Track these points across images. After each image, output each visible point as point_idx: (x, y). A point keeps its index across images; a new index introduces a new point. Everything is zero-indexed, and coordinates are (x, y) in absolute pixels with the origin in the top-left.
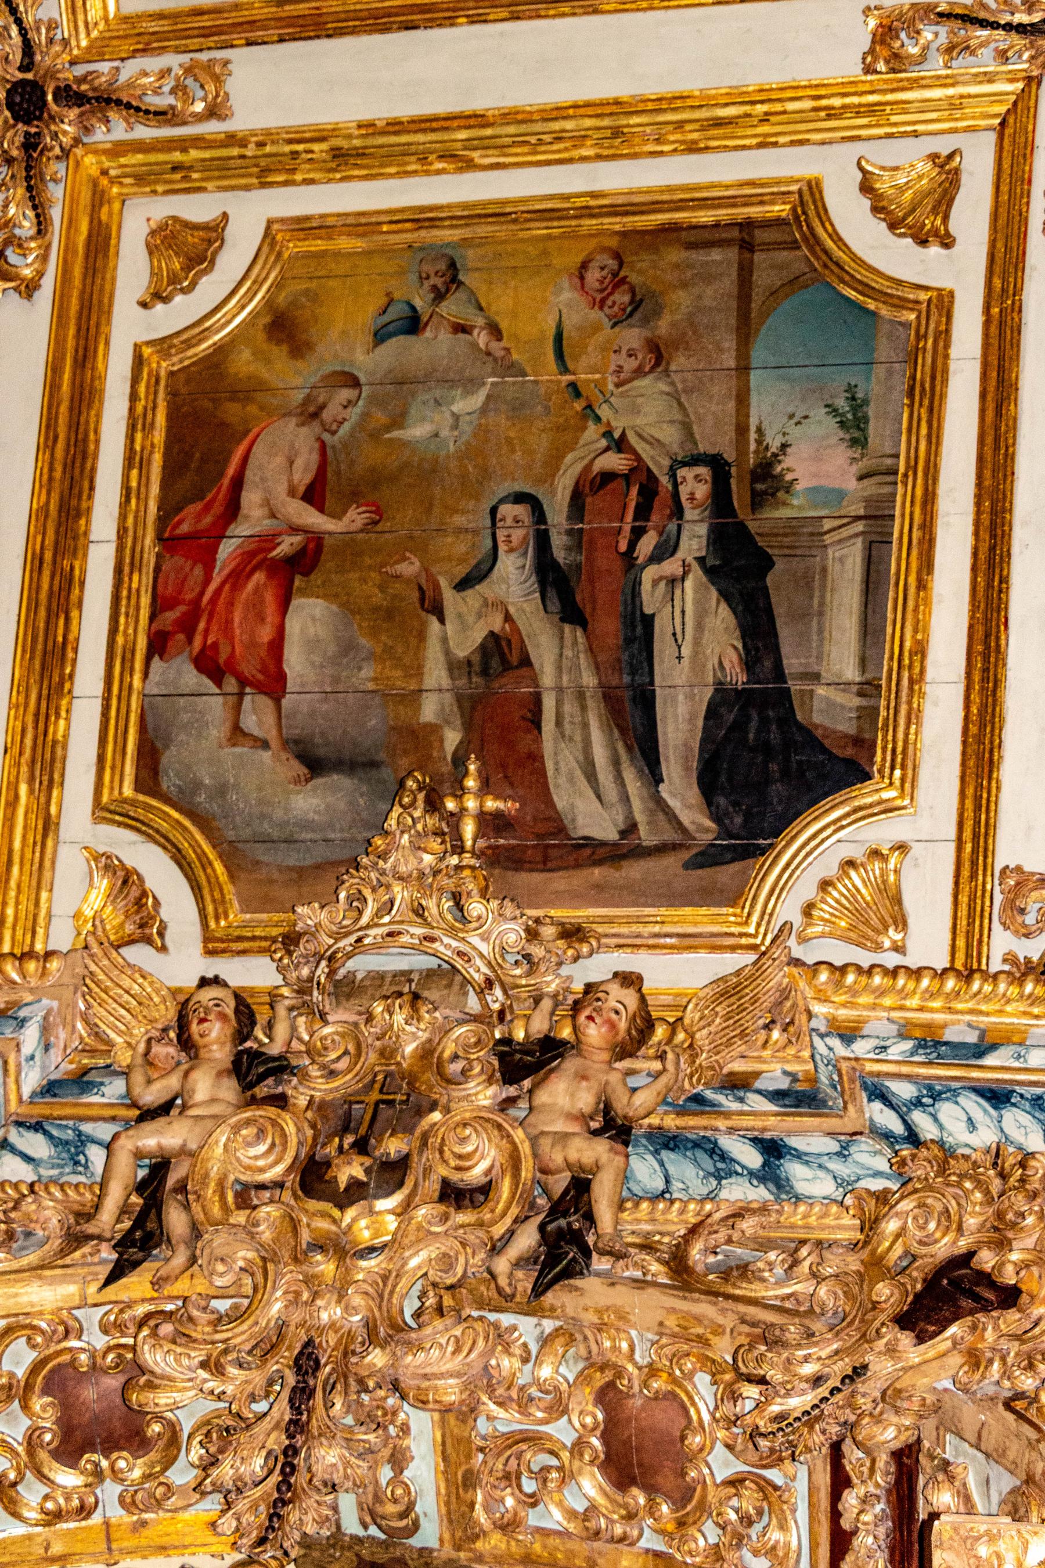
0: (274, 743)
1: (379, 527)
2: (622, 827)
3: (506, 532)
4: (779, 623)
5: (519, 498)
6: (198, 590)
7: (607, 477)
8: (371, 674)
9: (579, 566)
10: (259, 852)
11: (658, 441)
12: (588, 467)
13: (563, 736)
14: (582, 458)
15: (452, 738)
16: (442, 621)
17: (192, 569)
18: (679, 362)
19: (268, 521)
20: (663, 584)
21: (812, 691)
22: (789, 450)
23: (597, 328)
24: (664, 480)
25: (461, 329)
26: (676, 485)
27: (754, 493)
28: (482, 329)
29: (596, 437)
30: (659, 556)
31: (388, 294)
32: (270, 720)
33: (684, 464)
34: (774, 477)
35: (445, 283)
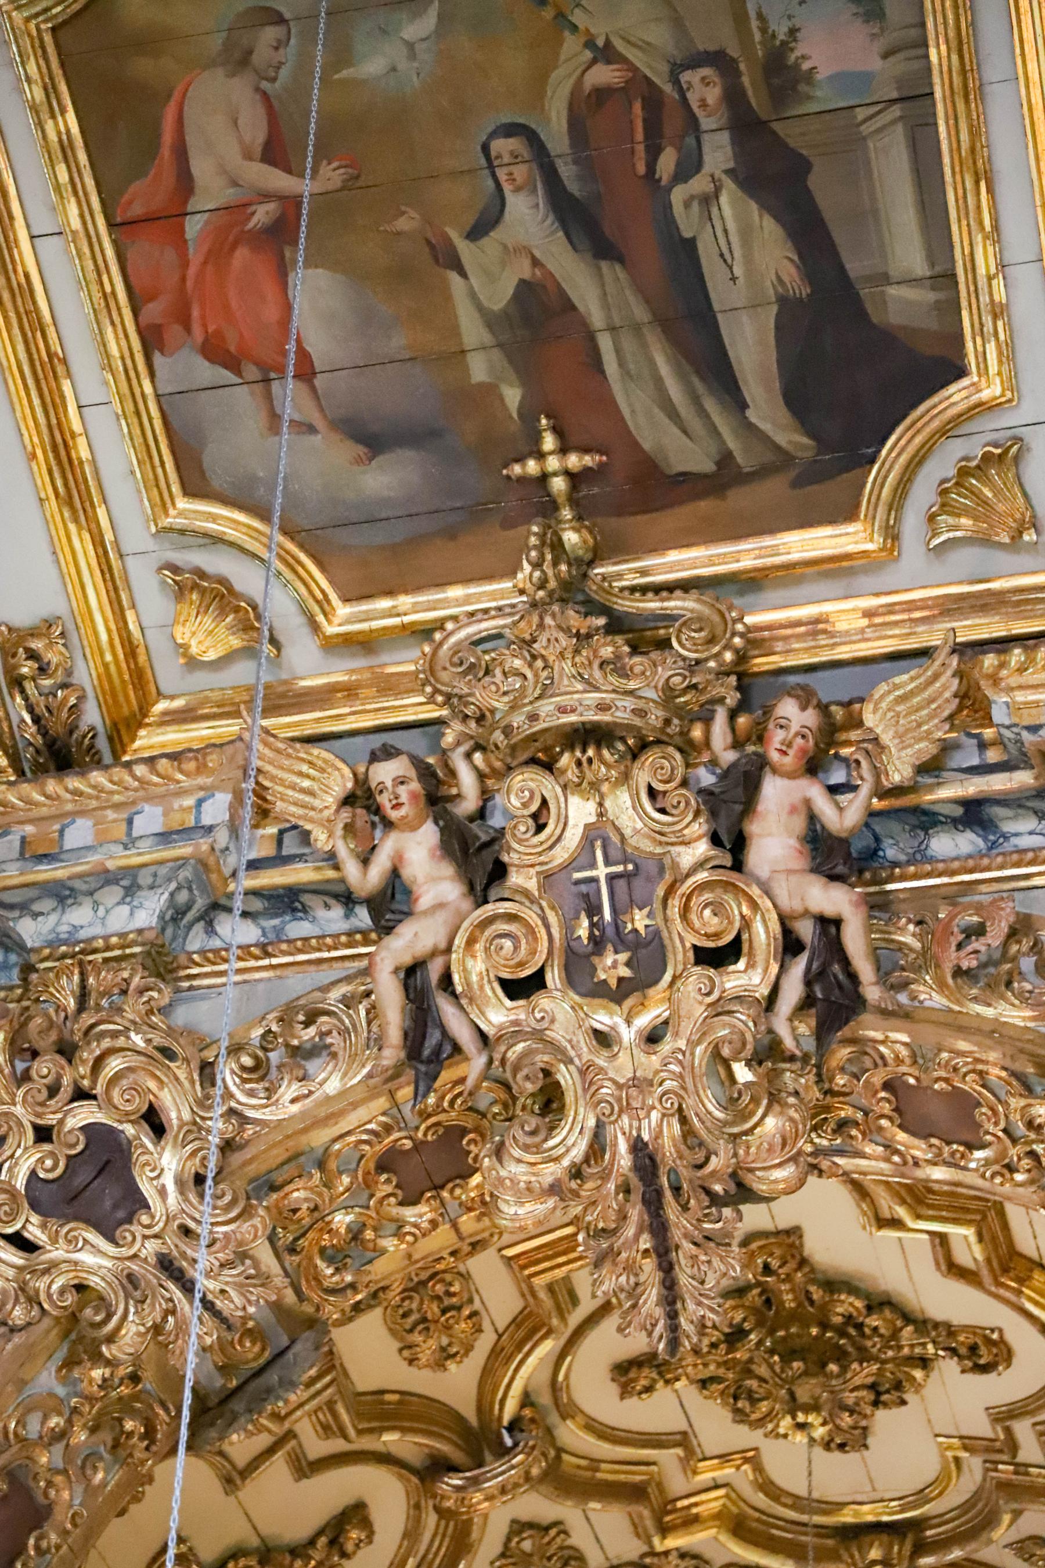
2: (717, 458)
3: (505, 170)
5: (510, 130)
6: (176, 277)
7: (601, 95)
8: (403, 342)
10: (343, 536)
11: (648, 44)
13: (631, 377)
14: (570, 75)
15: (512, 396)
19: (232, 191)
20: (695, 206)
24: (668, 88)
26: (682, 93)
29: (578, 48)
30: (683, 174)
34: (787, 67)
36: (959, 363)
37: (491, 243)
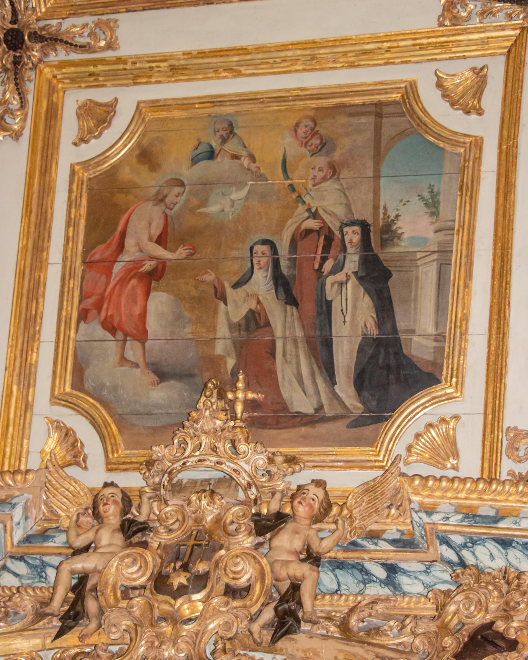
0: (142, 364)
1: (194, 257)
2: (316, 407)
3: (258, 259)
4: (395, 305)
5: (265, 242)
6: (103, 288)
7: (308, 232)
8: (190, 330)
9: (294, 277)
10: (134, 420)
11: (334, 213)
12: (299, 227)
13: (286, 362)
14: (296, 222)
15: (231, 362)
16: (226, 304)
17: (100, 278)
18: (344, 174)
19: (138, 254)
20: (336, 285)
21: (411, 339)
22: (400, 218)
23: (303, 157)
24: (337, 233)
25: (236, 157)
26: (343, 235)
27: (382, 240)
28: (246, 157)
29: (303, 211)
31: (198, 139)
32: (140, 353)
33: (347, 225)
34: (392, 231)
35: (227, 134)
36: (439, 378)
37: (241, 291)
